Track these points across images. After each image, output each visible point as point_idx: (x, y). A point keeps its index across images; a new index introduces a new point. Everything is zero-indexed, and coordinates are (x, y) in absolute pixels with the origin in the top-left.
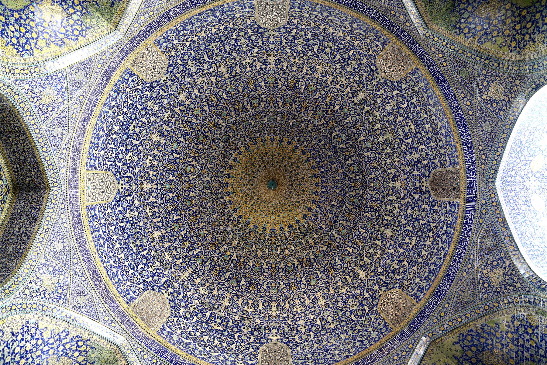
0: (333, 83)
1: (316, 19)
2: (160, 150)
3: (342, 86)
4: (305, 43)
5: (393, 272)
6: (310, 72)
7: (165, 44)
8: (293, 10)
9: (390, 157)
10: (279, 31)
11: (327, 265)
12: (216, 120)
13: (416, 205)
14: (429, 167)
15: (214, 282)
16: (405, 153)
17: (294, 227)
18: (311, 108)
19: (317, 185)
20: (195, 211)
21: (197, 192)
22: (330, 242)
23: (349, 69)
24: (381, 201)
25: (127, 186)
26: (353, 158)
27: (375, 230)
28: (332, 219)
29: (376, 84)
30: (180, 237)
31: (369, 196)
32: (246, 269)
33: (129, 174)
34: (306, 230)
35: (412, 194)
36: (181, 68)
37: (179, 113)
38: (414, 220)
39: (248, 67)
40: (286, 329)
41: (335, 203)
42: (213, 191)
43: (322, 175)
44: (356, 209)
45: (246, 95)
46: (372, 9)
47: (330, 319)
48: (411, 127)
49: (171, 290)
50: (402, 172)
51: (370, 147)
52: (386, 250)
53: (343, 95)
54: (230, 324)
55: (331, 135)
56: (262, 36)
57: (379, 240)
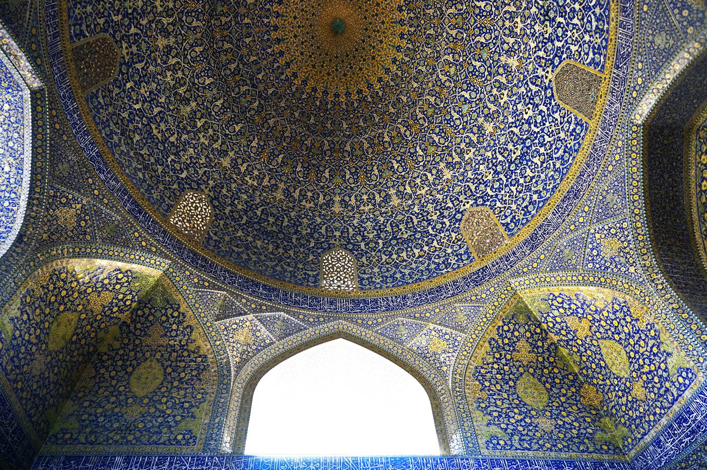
0: (261, 176)
1: (289, 260)
4: (299, 229)
6: (292, 190)
8: (315, 273)
10: (330, 244)
13: (131, 16)
14: (123, 79)
16: (159, 92)
19: (276, 28)
24: (182, 12)
39: (365, 200)
45: (369, 162)
46: (229, 283)
48: (157, 130)
50: (159, 61)
53: (248, 161)
55: (260, 103)
56: (349, 239)
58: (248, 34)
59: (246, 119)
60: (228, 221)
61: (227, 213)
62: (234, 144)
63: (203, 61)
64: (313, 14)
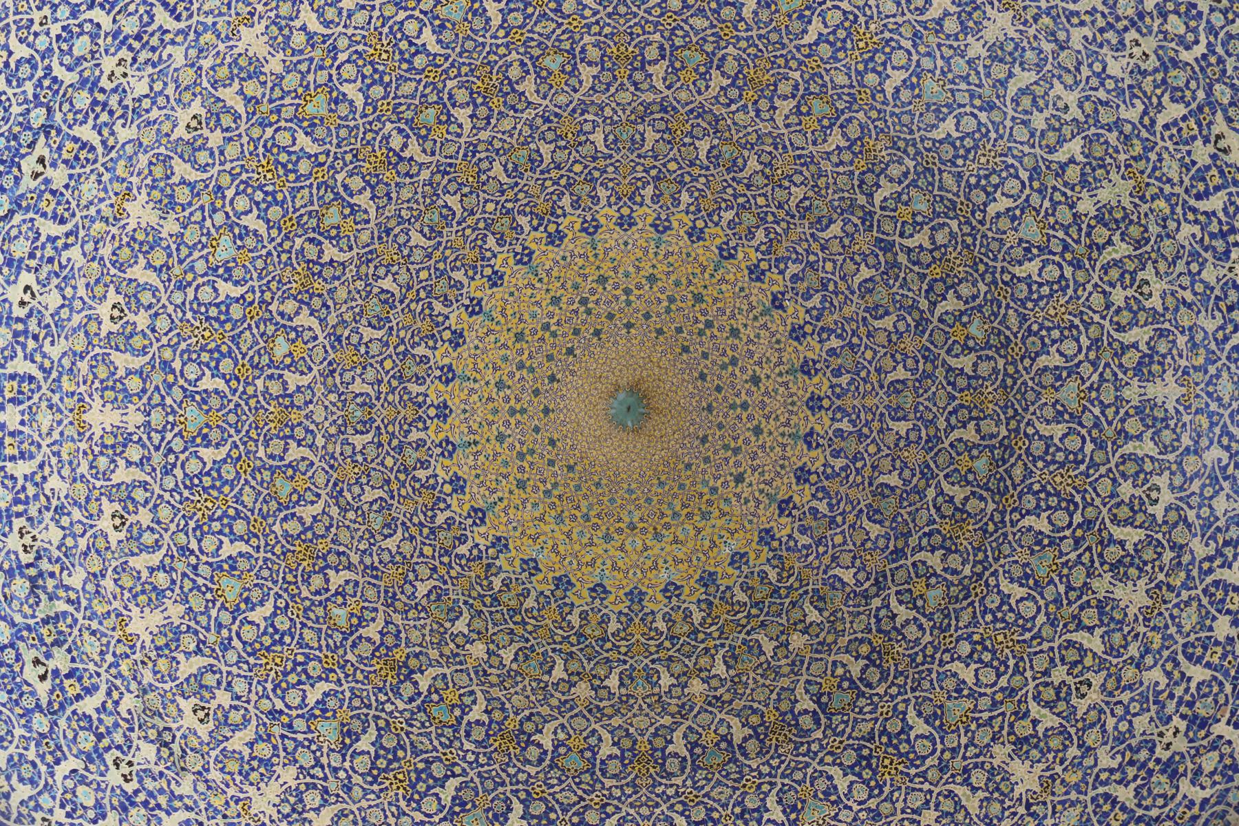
2: (158, 264)
11: (871, 738)
18: (785, 88)
19: (814, 404)
20: (308, 521)
21: (320, 441)
22: (878, 641)
24: (1094, 465)
26: (965, 290)
27: (1070, 588)
28: (882, 543)
30: (249, 633)
31: (1038, 447)
32: (528, 762)
34: (776, 591)
41: (893, 480)
42: (385, 438)
43: (836, 362)
44: (982, 498)
48: (1222, 144)
50: (1182, 340)
51: (1037, 239)
55: (871, 195)
57: (1090, 630)
58: (898, 392)
59: (918, 153)
62: (965, 79)
63: (1041, 327)
64: (704, 440)
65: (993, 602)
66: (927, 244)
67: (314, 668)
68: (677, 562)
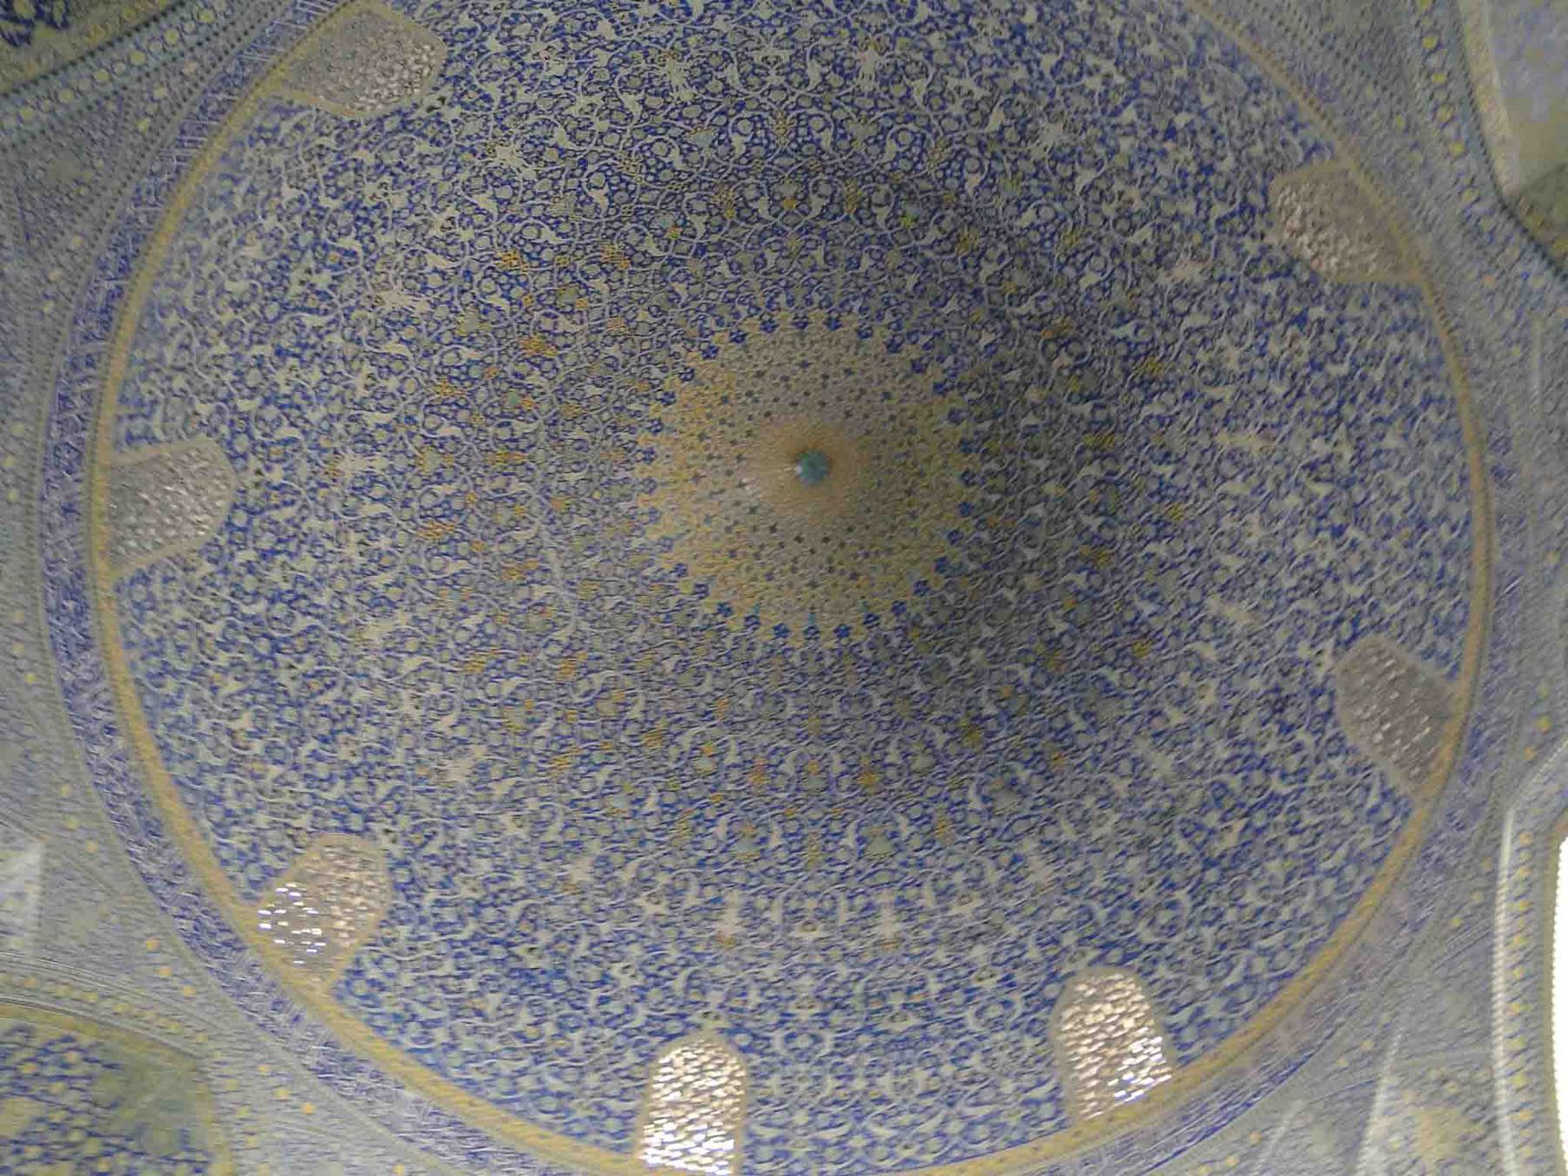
1: (196, 343)
3: (464, 220)
5: (1207, 169)
7: (269, 859)
8: (158, 433)
9: (760, 71)
12: (554, 650)
13: (960, 18)
15: (1085, 776)
16: (743, 21)
17: (970, 436)
18: (547, 324)
21: (783, 743)
23: (398, 200)
24: (929, 127)
25: (715, 997)
26: (751, 193)
29: (458, 109)
31: (904, 165)
33: (678, 984)
34: (989, 398)
35: (915, 21)
36: (359, 783)
37: (510, 782)
38: (1018, 41)
40: (1309, 605)
41: (912, 280)
43: (799, 301)
47: (1320, 447)
49: (1069, 939)
50: (823, 41)
51: (713, 134)
52: (1119, 161)
53: (501, 214)
54: (1235, 783)
57: (1074, 174)
60: (330, 159)
61: (356, 155)
62: (555, 181)
65: (1035, 237)
66: (705, 218)
67: (955, 796)
68: (944, 466)
